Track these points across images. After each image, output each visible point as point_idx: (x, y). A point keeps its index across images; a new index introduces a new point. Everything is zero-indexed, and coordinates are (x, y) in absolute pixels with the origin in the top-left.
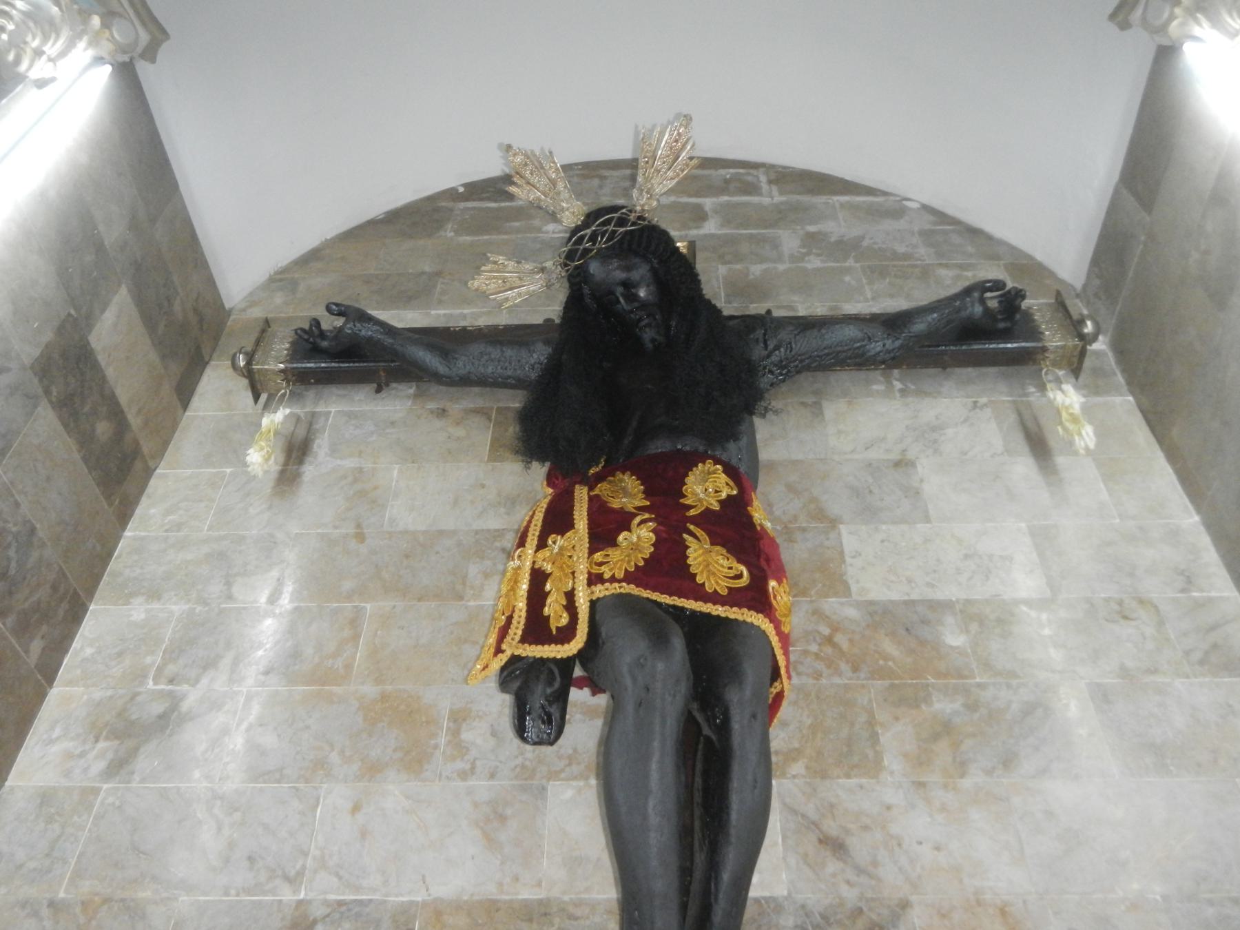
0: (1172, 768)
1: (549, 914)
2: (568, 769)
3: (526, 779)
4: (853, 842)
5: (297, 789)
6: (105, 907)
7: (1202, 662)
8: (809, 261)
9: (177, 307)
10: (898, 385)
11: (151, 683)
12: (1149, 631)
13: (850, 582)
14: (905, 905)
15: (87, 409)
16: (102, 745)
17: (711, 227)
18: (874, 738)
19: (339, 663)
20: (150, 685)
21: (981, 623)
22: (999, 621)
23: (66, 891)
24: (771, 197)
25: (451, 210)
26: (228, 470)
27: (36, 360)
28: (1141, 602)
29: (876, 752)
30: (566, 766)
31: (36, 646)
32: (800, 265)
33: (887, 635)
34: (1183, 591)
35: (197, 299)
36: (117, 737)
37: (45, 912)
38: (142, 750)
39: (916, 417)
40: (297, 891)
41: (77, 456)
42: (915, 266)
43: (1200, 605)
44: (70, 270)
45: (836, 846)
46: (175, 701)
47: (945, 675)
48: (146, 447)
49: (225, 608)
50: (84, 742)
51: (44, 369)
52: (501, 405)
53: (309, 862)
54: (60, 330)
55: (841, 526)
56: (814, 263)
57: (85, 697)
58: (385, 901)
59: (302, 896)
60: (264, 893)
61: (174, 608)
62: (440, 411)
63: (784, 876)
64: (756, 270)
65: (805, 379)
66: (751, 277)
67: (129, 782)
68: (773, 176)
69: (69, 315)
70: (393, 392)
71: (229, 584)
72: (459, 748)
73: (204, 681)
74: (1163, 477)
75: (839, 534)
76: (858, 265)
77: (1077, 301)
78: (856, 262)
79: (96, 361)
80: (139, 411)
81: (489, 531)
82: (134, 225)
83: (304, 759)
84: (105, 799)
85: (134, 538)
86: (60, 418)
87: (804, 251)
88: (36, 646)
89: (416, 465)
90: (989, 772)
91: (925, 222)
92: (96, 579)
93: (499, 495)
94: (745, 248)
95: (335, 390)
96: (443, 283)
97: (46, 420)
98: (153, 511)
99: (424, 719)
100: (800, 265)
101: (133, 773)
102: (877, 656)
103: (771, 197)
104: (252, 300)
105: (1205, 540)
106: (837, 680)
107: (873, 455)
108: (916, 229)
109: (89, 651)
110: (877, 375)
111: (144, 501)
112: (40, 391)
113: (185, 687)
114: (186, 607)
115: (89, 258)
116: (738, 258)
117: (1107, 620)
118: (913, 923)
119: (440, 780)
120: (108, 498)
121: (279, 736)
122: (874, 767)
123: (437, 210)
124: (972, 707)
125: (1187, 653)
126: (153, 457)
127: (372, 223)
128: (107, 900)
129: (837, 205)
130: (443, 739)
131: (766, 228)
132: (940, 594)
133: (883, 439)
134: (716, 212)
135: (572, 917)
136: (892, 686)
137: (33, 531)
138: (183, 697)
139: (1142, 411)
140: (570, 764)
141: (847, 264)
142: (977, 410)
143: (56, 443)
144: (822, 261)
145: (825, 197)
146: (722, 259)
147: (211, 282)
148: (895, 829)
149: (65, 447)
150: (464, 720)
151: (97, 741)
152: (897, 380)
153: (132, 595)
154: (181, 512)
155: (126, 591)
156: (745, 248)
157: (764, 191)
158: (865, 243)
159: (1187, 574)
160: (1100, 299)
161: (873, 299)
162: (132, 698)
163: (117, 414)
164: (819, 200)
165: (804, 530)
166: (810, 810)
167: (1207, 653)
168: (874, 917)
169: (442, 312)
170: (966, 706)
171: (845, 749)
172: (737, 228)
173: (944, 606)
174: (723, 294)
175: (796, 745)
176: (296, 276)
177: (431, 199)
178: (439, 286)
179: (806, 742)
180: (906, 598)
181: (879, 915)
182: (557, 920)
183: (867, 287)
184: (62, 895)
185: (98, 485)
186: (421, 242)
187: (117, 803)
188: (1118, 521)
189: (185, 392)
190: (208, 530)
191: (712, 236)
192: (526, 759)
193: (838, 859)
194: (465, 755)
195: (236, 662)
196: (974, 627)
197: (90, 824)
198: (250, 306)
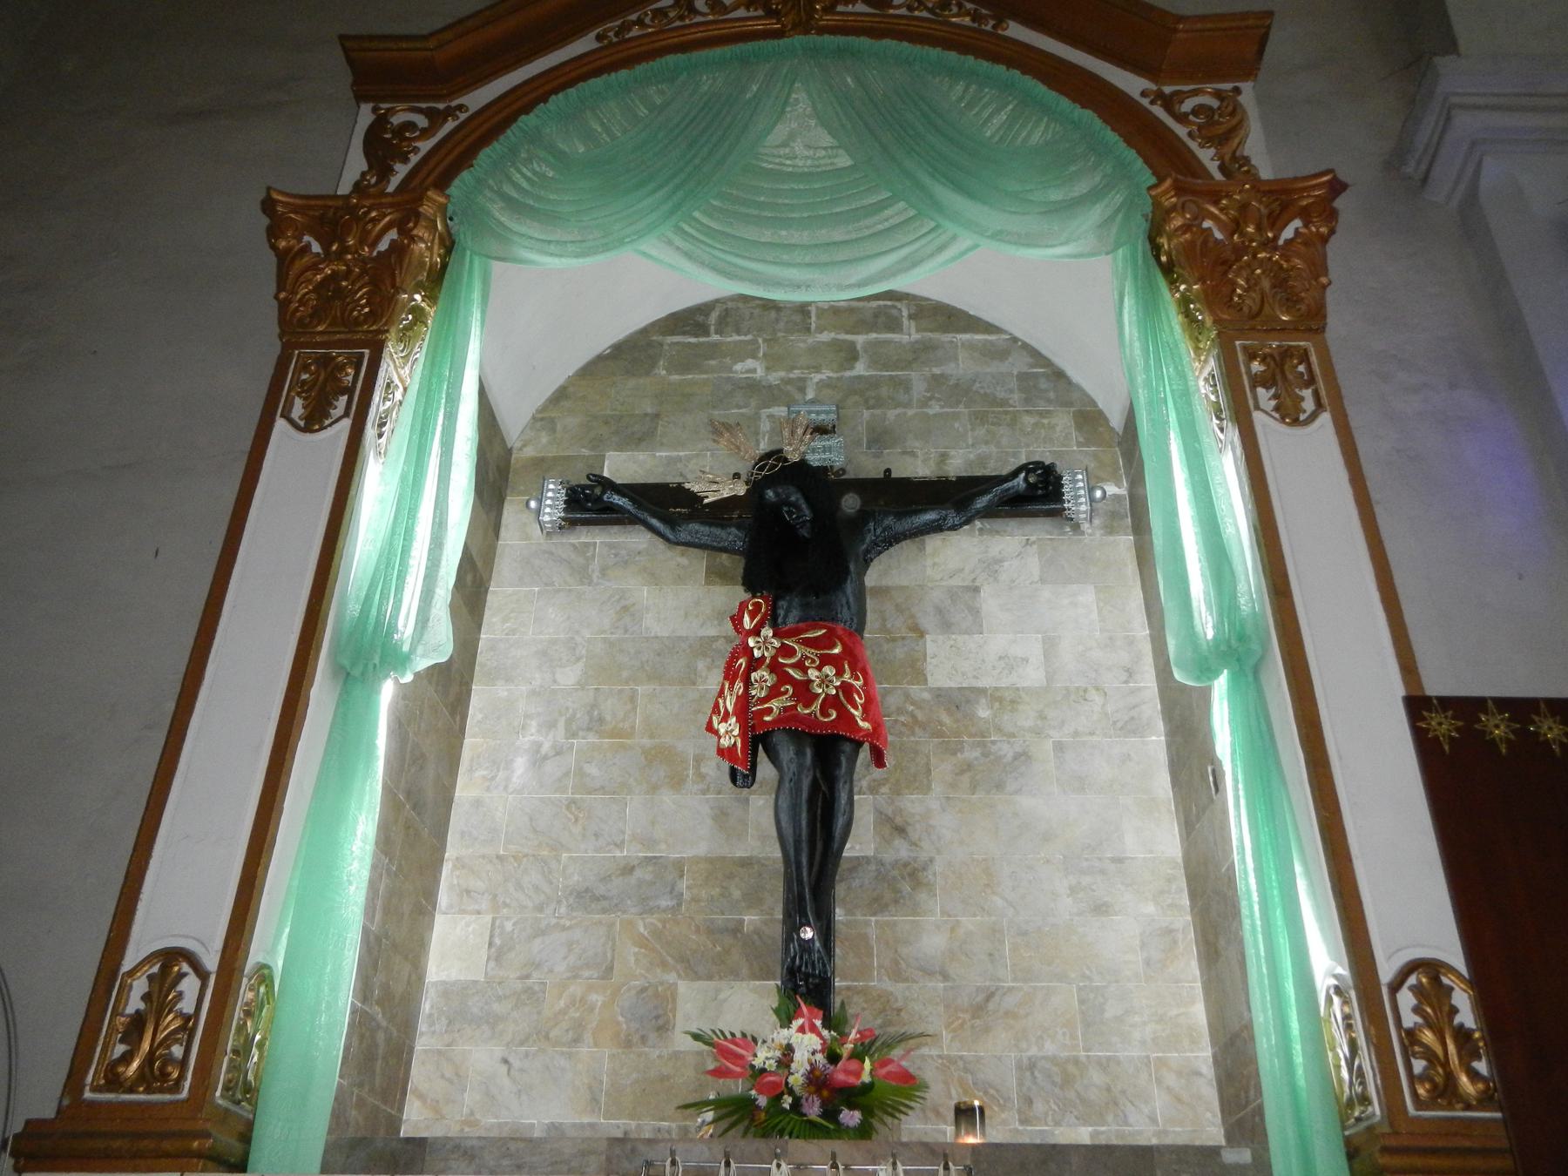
4: (909, 829)
6: (525, 859)
7: (1121, 729)
8: (930, 407)
14: (931, 860)
16: (500, 773)
17: (860, 369)
19: (627, 725)
21: (1001, 703)
22: (1013, 702)
24: (910, 334)
37: (495, 861)
40: (622, 852)
42: (1006, 413)
43: (1133, 692)
45: (901, 831)
61: (524, 688)
72: (701, 777)
77: (1117, 449)
87: (929, 395)
88: (458, 718)
94: (884, 391)
95: (596, 529)
98: (494, 620)
103: (910, 334)
106: (912, 739)
107: (956, 582)
108: (1015, 373)
109: (480, 716)
116: (879, 403)
122: (927, 789)
123: (650, 344)
124: (985, 755)
125: (1115, 723)
127: (600, 359)
128: (526, 856)
131: (902, 369)
132: (980, 684)
133: (963, 569)
135: (763, 865)
142: (1028, 547)
144: (942, 407)
145: (951, 335)
151: (498, 771)
156: (884, 391)
161: (973, 445)
164: (947, 337)
165: (903, 638)
166: (890, 813)
169: (664, 454)
173: (982, 691)
174: (865, 439)
176: (553, 415)
177: (645, 331)
178: (659, 428)
182: (756, 867)
184: (502, 852)
191: (859, 377)
196: (997, 705)
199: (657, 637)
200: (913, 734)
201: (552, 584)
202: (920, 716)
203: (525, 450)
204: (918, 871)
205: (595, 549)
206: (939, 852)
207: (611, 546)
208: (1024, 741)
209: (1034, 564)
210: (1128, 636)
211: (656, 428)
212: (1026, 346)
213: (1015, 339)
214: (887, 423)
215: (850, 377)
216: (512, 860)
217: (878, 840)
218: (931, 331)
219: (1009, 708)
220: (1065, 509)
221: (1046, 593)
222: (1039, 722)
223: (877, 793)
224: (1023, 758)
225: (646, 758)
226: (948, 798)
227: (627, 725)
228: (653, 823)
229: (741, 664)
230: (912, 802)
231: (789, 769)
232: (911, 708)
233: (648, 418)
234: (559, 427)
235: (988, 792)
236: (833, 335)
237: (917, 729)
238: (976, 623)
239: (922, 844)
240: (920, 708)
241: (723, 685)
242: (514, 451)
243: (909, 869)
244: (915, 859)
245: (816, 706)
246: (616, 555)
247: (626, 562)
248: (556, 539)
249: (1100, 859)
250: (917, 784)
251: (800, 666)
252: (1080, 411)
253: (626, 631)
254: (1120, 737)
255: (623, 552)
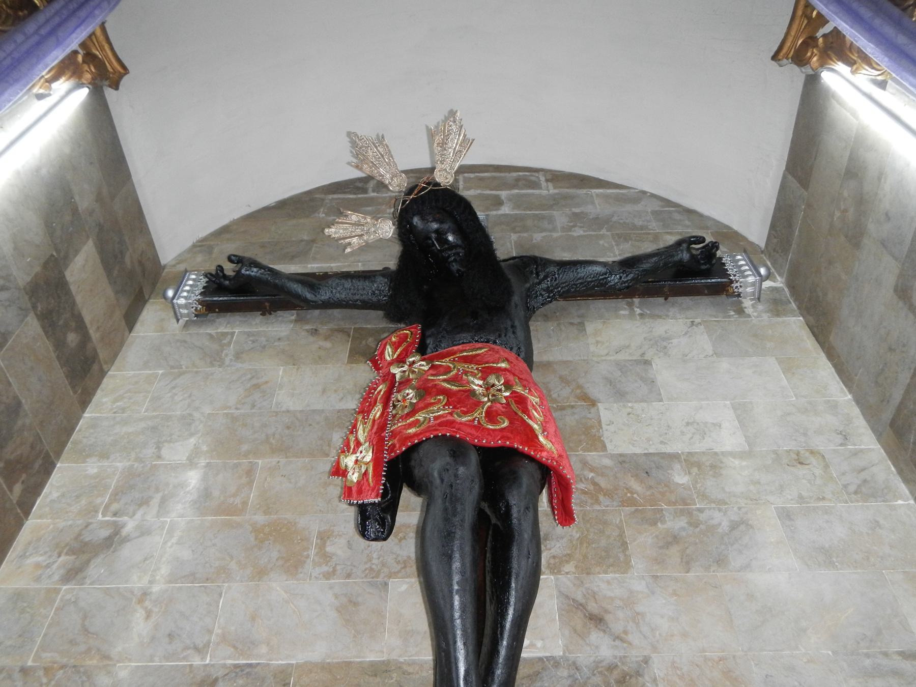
0: (836, 564)
1: (389, 671)
2: (403, 570)
3: (373, 578)
4: (608, 617)
5: (205, 587)
6: (61, 671)
7: (856, 493)
9: (127, 260)
10: (638, 311)
11: (100, 515)
12: (818, 472)
13: (606, 441)
14: (646, 660)
15: (61, 322)
16: (62, 558)
17: (506, 210)
18: (624, 545)
19: (238, 500)
20: (100, 517)
22: (713, 467)
23: (34, 661)
24: (548, 190)
25: (323, 200)
26: (161, 372)
27: (28, 284)
28: (812, 452)
29: (625, 555)
30: (402, 568)
31: (18, 488)
32: (570, 233)
33: (632, 477)
34: (841, 445)
35: (141, 255)
36: (74, 554)
37: (17, 675)
38: (92, 562)
39: (651, 331)
40: (203, 659)
41: (53, 355)
42: (649, 234)
43: (855, 454)
44: (54, 224)
45: (597, 620)
46: (117, 529)
47: (674, 503)
48: (102, 354)
49: (155, 465)
50: (50, 556)
51: (34, 290)
52: (357, 326)
53: (213, 637)
54: (45, 265)
55: (599, 404)
56: (578, 232)
57: (51, 527)
58: (268, 664)
59: (207, 662)
60: (179, 660)
62: (313, 331)
63: (560, 642)
64: (538, 237)
65: (574, 308)
66: (534, 241)
67: (82, 584)
68: (549, 177)
69: (52, 255)
70: (280, 318)
71: (159, 448)
72: (326, 557)
73: (138, 515)
74: (825, 370)
75: (598, 409)
76: (608, 233)
78: (607, 231)
79: (69, 289)
80: (98, 328)
81: (348, 410)
82: (99, 199)
83: (211, 566)
84: (63, 596)
85: (92, 419)
86: (43, 328)
87: (572, 224)
88: (18, 488)
89: (296, 367)
90: (707, 569)
91: (656, 206)
92: (63, 445)
93: (355, 386)
95: (237, 318)
96: (316, 247)
97: (33, 325)
98: (104, 400)
99: (299, 538)
100: (570, 233)
101: (85, 578)
102: (625, 491)
103: (548, 190)
104: (180, 260)
105: (856, 411)
106: (597, 507)
107: (622, 357)
108: (650, 210)
109: (55, 495)
110: (622, 303)
111: (99, 393)
112: (29, 305)
113: (126, 518)
114: (128, 464)
115: (68, 218)
116: (525, 229)
117: (788, 465)
118: (655, 673)
119: (310, 580)
120: (73, 387)
121: (193, 551)
122: (625, 566)
123: (312, 200)
125: (845, 486)
126: (106, 363)
127: (267, 209)
128: (63, 667)
129: (594, 195)
130: (313, 552)
132: (669, 449)
133: (628, 347)
134: (510, 200)
136: (636, 510)
137: (19, 404)
138: (124, 525)
139: (809, 327)
140: (405, 567)
141: (601, 233)
142: (694, 327)
143: (39, 344)
144: (584, 231)
146: (514, 230)
147: (151, 244)
148: (639, 608)
149: (45, 346)
150: (328, 538)
151: (59, 556)
152: (637, 308)
153: (89, 456)
154: (126, 400)
155: (84, 454)
156: (529, 223)
157: (543, 186)
158: (615, 219)
159: (844, 434)
160: (777, 252)
162: (87, 526)
163: (81, 327)
165: (573, 407)
166: (579, 597)
167: (859, 486)
168: (626, 668)
170: (690, 524)
171: (603, 554)
172: (524, 210)
175: (569, 552)
176: (212, 243)
178: (314, 249)
179: (576, 549)
180: (646, 452)
181: (629, 667)
182: (394, 675)
183: (615, 247)
184: (30, 663)
185: (67, 377)
186: (302, 221)
187: (73, 600)
188: (794, 399)
189: (131, 319)
190: (144, 412)
192: (373, 564)
193: (599, 629)
194: (329, 561)
195: (163, 501)
196: (695, 470)
197: (52, 613)
198: (178, 263)
199: (288, 411)
200: (597, 501)
201: (180, 367)
202: (603, 483)
203: (178, 266)
204: (631, 677)
205: (233, 337)
206: (655, 649)
207: (249, 334)
208: (739, 508)
209: (703, 341)
210: (829, 401)
211: (310, 249)
212: (653, 196)
213: (644, 193)
214: (534, 241)
215: (496, 215)
216: (41, 673)
217: (567, 632)
218: (568, 188)
219: (711, 473)
220: (732, 282)
221: (724, 364)
222: (752, 487)
223: (559, 572)
224: (743, 527)
225: (256, 539)
226: (655, 577)
227: (238, 500)
228: (253, 619)
229: (381, 391)
230: (608, 582)
231: (442, 480)
232: (591, 475)
233: (303, 243)
234: (216, 250)
235: (707, 569)
236: (479, 192)
237: (601, 498)
238: (653, 391)
239: (630, 637)
240: (603, 475)
241: (356, 420)
242: (168, 267)
243: (616, 674)
244: (623, 659)
245: (479, 414)
246: (253, 342)
247: (264, 347)
248: (194, 330)
249: (886, 654)
250: (611, 560)
251: (455, 380)
252: (716, 232)
253: (253, 406)
254: (858, 501)
255: (263, 339)
